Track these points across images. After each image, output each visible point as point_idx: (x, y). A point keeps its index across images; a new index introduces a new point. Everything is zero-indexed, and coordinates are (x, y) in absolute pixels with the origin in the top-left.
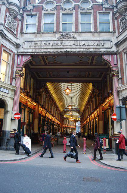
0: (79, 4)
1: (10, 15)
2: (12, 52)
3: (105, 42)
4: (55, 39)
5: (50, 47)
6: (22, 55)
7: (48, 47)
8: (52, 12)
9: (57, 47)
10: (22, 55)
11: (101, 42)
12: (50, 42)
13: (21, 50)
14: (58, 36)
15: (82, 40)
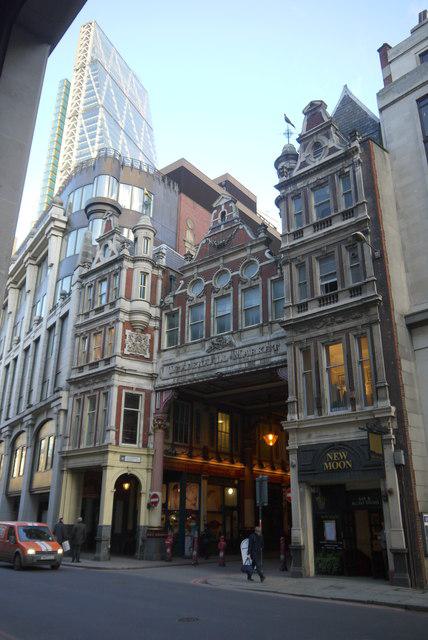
0: (239, 272)
1: (134, 330)
2: (143, 390)
3: (280, 341)
4: (203, 353)
5: (197, 370)
6: (162, 391)
7: (194, 371)
8: (200, 301)
9: (206, 368)
10: (162, 391)
11: (273, 343)
12: (197, 360)
13: (159, 383)
14: (207, 345)
15: (243, 347)
